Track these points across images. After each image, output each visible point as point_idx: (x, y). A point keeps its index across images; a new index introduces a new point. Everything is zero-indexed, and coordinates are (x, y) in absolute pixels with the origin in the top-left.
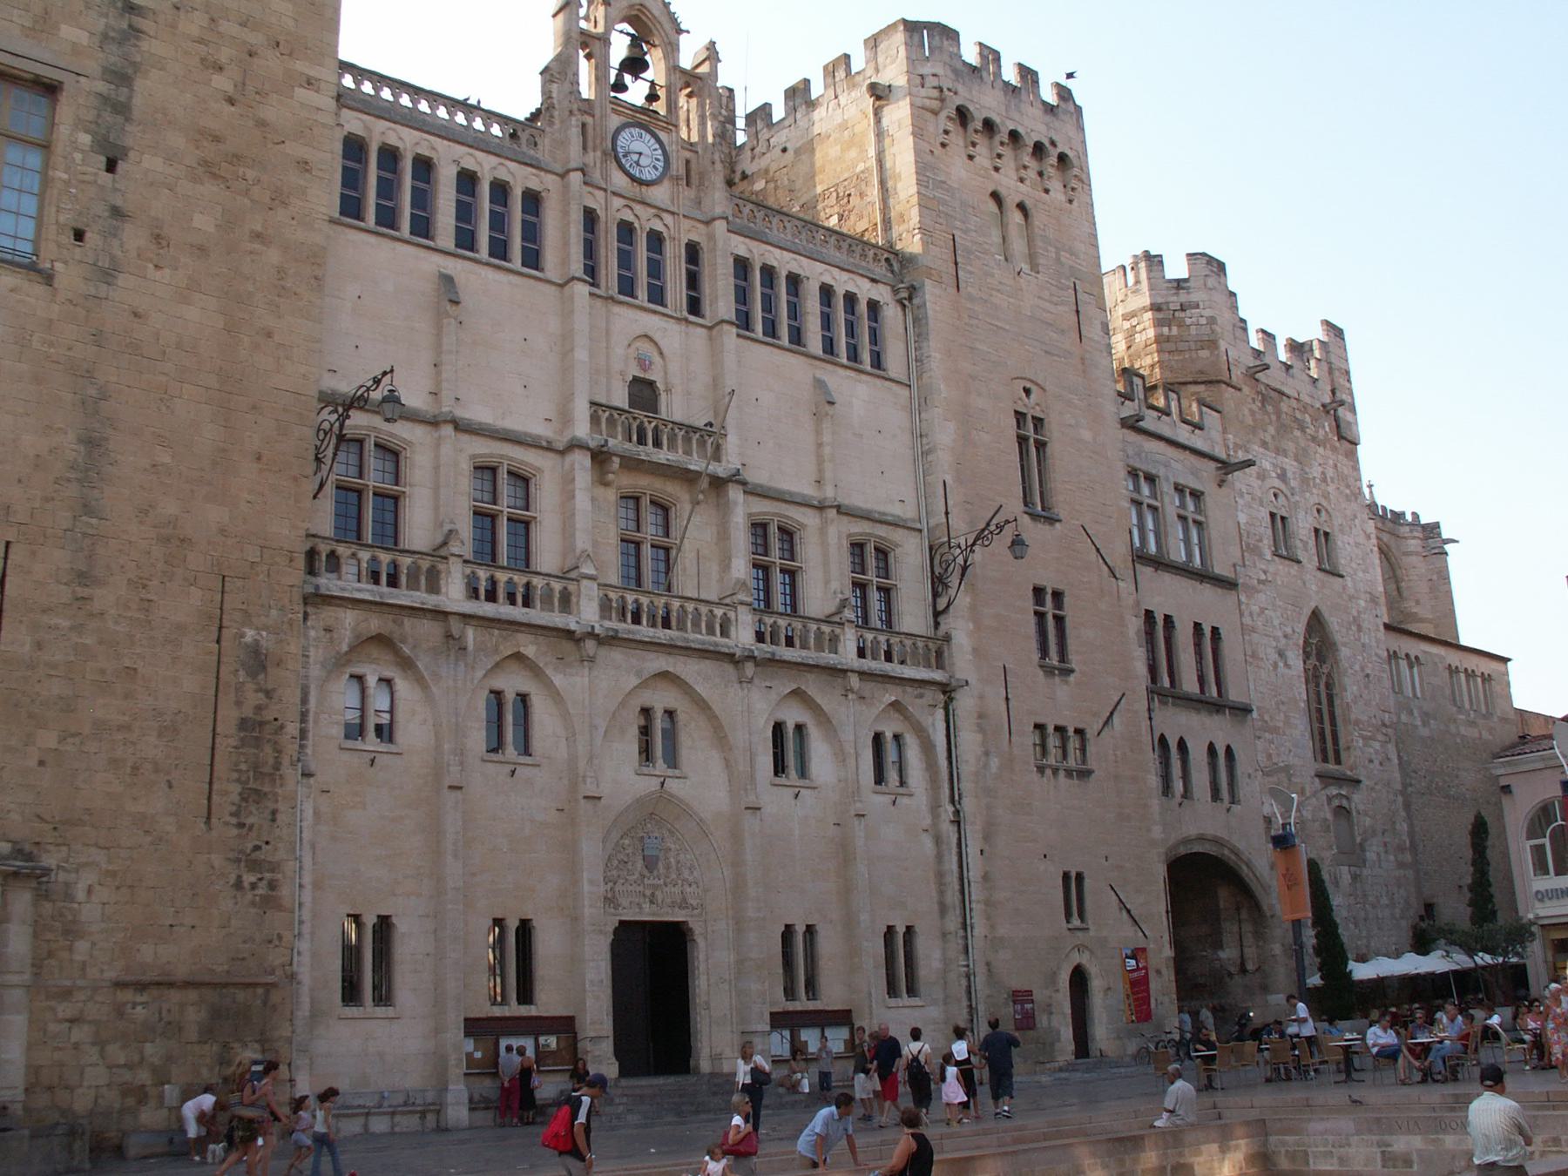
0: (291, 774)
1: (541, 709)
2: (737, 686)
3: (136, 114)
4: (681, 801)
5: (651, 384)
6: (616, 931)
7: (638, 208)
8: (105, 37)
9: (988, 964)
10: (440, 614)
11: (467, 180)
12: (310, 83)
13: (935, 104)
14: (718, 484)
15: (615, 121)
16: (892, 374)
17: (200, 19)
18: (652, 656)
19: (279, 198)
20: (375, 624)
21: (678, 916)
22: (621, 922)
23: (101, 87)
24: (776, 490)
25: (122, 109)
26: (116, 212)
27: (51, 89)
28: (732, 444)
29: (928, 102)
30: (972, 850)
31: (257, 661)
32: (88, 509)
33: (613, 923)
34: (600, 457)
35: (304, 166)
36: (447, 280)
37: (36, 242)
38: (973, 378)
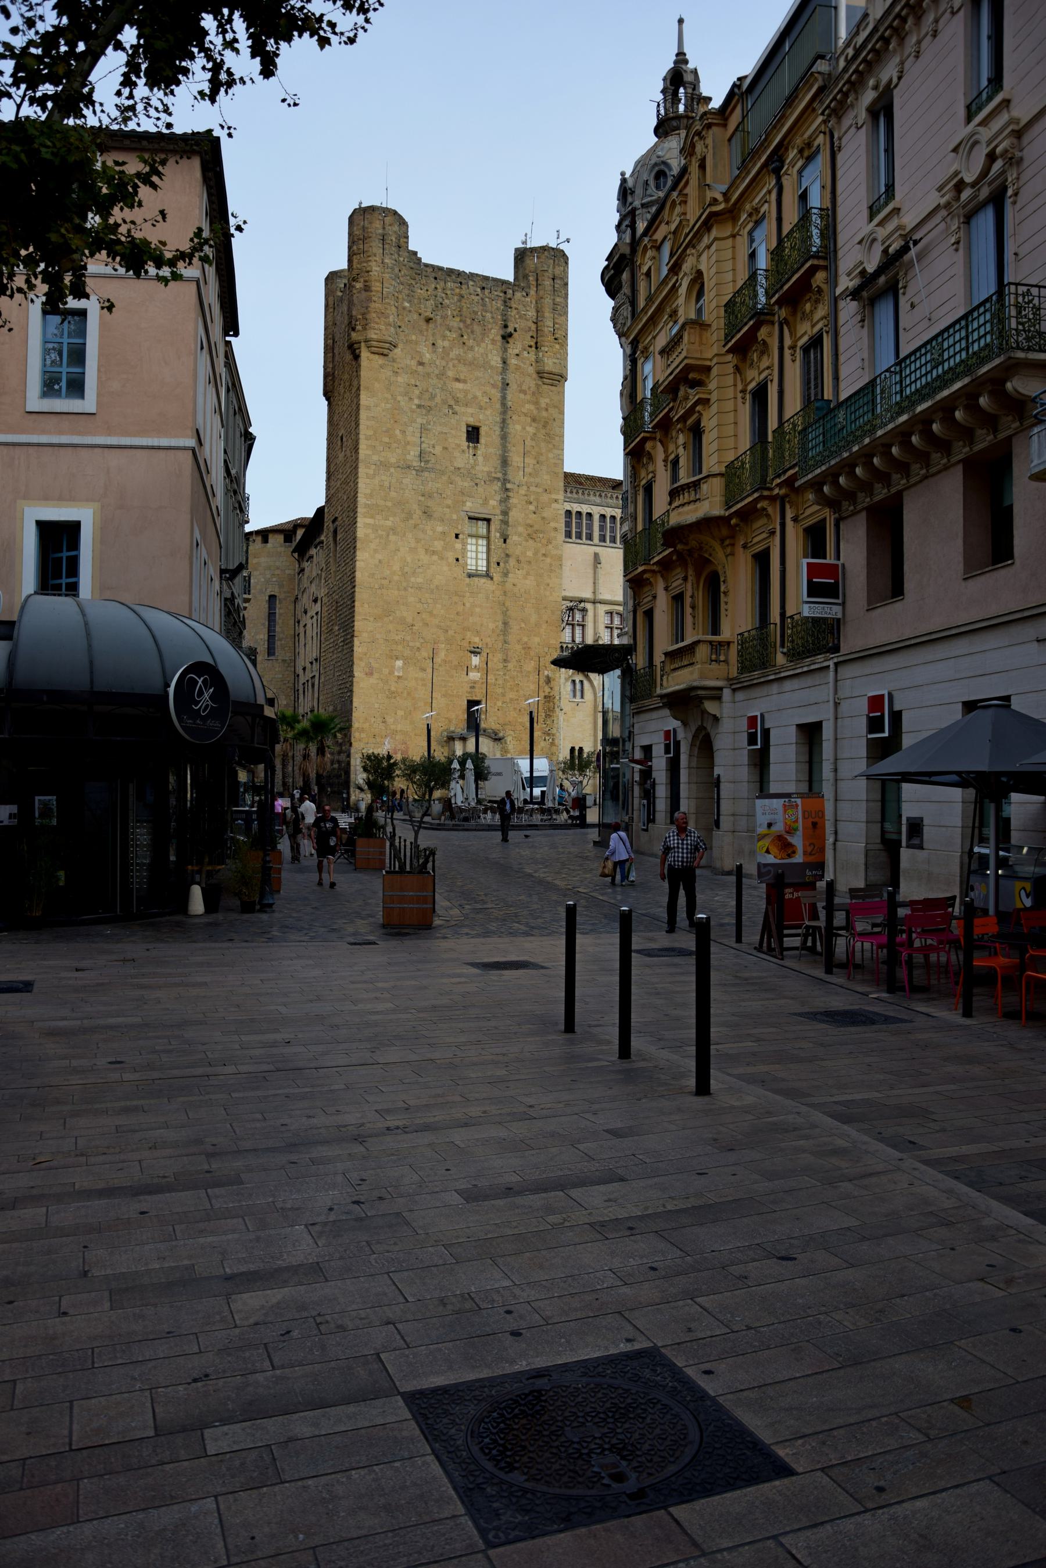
0: (557, 710)
11: (603, 517)
17: (525, 488)
19: (549, 542)
23: (501, 517)
25: (505, 523)
26: (507, 555)
27: (488, 521)
32: (505, 642)
35: (556, 529)
36: (596, 555)
37: (488, 566)
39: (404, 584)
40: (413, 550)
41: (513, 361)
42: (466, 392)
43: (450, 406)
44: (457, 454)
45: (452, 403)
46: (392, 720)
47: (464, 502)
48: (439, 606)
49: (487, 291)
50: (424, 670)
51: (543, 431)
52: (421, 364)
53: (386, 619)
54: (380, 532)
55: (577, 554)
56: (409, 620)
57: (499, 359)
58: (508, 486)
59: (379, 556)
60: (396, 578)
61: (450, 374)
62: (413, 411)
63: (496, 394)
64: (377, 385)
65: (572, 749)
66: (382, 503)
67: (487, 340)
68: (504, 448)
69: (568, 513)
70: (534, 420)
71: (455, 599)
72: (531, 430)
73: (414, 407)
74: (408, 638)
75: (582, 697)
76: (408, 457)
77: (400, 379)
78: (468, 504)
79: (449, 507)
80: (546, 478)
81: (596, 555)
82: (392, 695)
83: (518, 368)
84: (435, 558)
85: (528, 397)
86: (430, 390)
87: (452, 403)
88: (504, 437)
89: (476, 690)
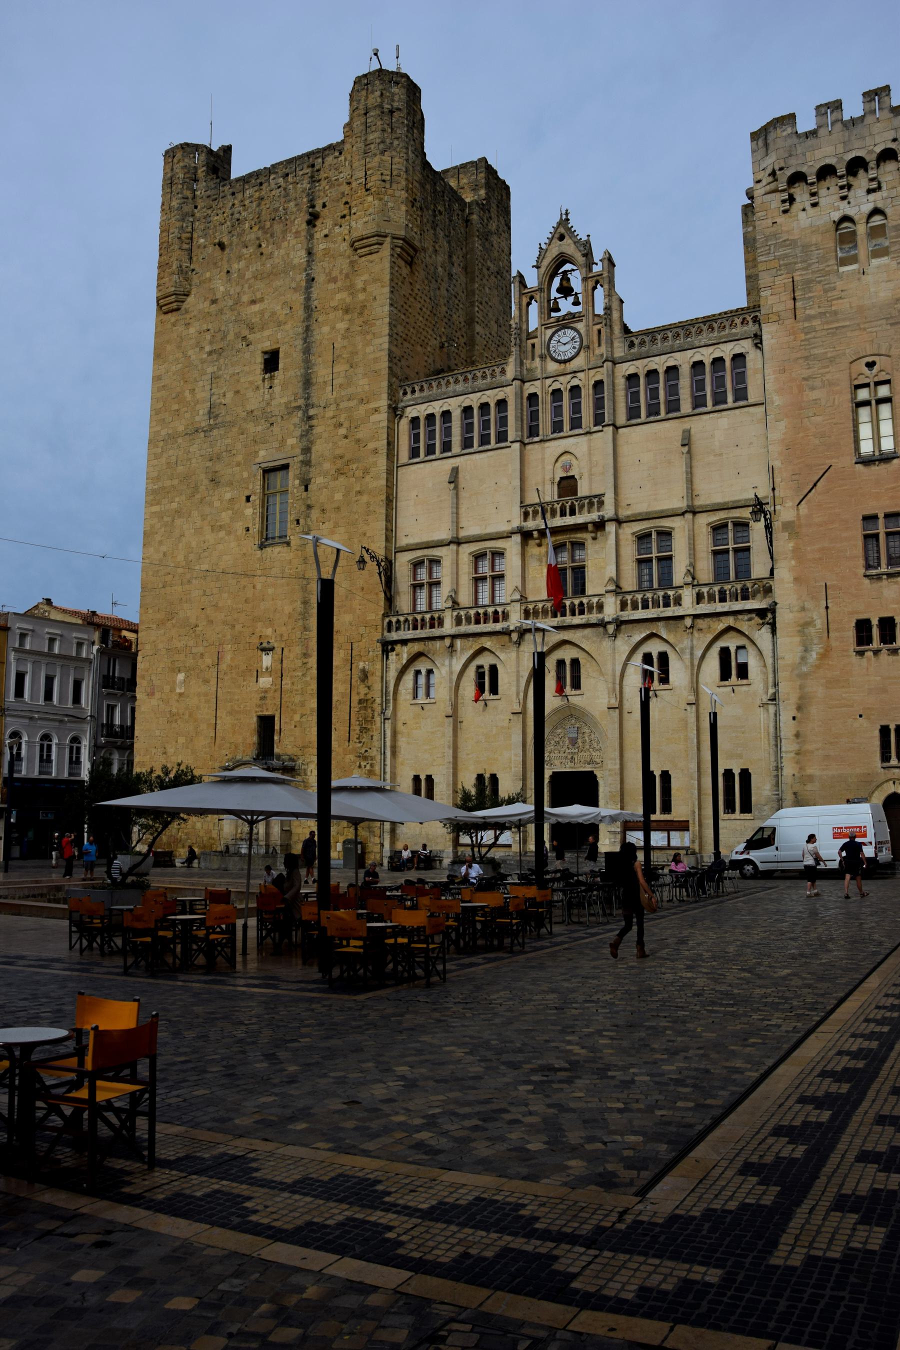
0: (378, 719)
3: (313, 462)
5: (573, 477)
7: (561, 379)
8: (302, 436)
9: (795, 794)
10: (442, 638)
12: (376, 410)
13: (773, 186)
14: (600, 525)
15: (549, 332)
16: (751, 400)
17: (333, 407)
19: (366, 471)
20: (416, 647)
21: (588, 768)
23: (301, 458)
24: (656, 512)
25: (307, 463)
26: (309, 507)
28: (609, 499)
29: (768, 188)
30: (786, 717)
31: (365, 676)
34: (526, 536)
35: (375, 451)
36: (455, 471)
38: (805, 379)
39: (188, 576)
40: (199, 531)
41: (320, 247)
42: (262, 313)
43: (244, 338)
44: (250, 394)
45: (245, 332)
46: (172, 750)
47: (257, 452)
48: (225, 595)
49: (290, 178)
50: (206, 681)
51: (359, 321)
52: (214, 302)
53: (169, 624)
54: (166, 519)
55: (423, 481)
56: (193, 621)
57: (303, 253)
58: (312, 412)
59: (164, 548)
60: (180, 570)
61: (245, 298)
62: (203, 362)
63: (298, 299)
64: (169, 348)
65: (417, 779)
66: (168, 483)
67: (290, 236)
68: (308, 364)
69: (415, 421)
70: (347, 311)
71: (244, 581)
72: (342, 326)
73: (205, 356)
74: (191, 643)
75: (428, 695)
76: (197, 419)
77: (192, 330)
78: (262, 453)
79: (238, 464)
80: (362, 384)
81: (455, 471)
82: (173, 717)
83: (327, 252)
84: (222, 534)
85: (339, 284)
86: (223, 328)
87: (245, 332)
88: (307, 351)
89: (268, 701)
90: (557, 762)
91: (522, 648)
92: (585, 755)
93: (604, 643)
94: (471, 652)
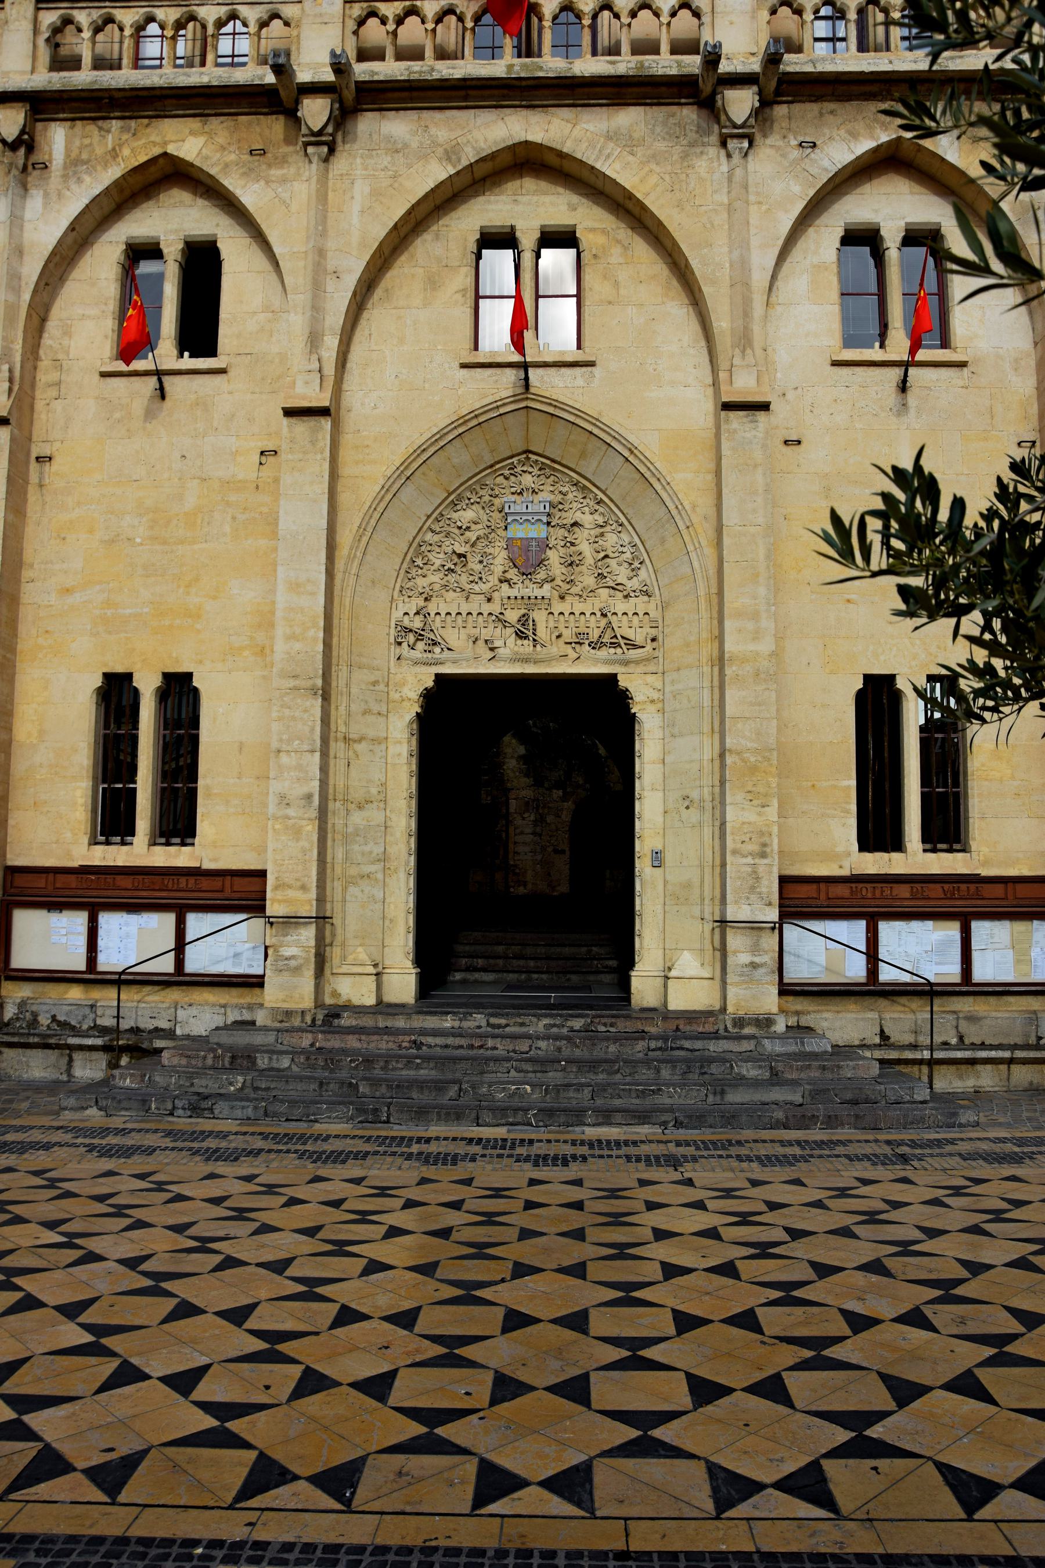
1: (237, 258)
2: (713, 151)
4: (579, 413)
6: (428, 696)
18: (485, 117)
21: (591, 664)
22: (439, 678)
33: (414, 682)
90: (454, 637)
91: (340, 163)
92: (582, 612)
93: (701, 165)
94: (113, 173)
